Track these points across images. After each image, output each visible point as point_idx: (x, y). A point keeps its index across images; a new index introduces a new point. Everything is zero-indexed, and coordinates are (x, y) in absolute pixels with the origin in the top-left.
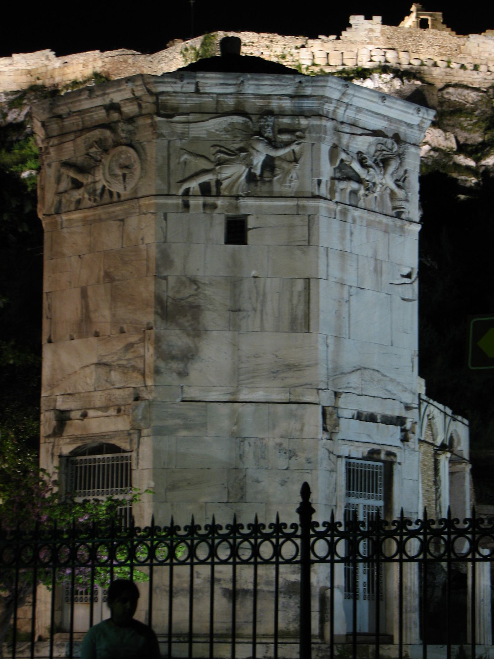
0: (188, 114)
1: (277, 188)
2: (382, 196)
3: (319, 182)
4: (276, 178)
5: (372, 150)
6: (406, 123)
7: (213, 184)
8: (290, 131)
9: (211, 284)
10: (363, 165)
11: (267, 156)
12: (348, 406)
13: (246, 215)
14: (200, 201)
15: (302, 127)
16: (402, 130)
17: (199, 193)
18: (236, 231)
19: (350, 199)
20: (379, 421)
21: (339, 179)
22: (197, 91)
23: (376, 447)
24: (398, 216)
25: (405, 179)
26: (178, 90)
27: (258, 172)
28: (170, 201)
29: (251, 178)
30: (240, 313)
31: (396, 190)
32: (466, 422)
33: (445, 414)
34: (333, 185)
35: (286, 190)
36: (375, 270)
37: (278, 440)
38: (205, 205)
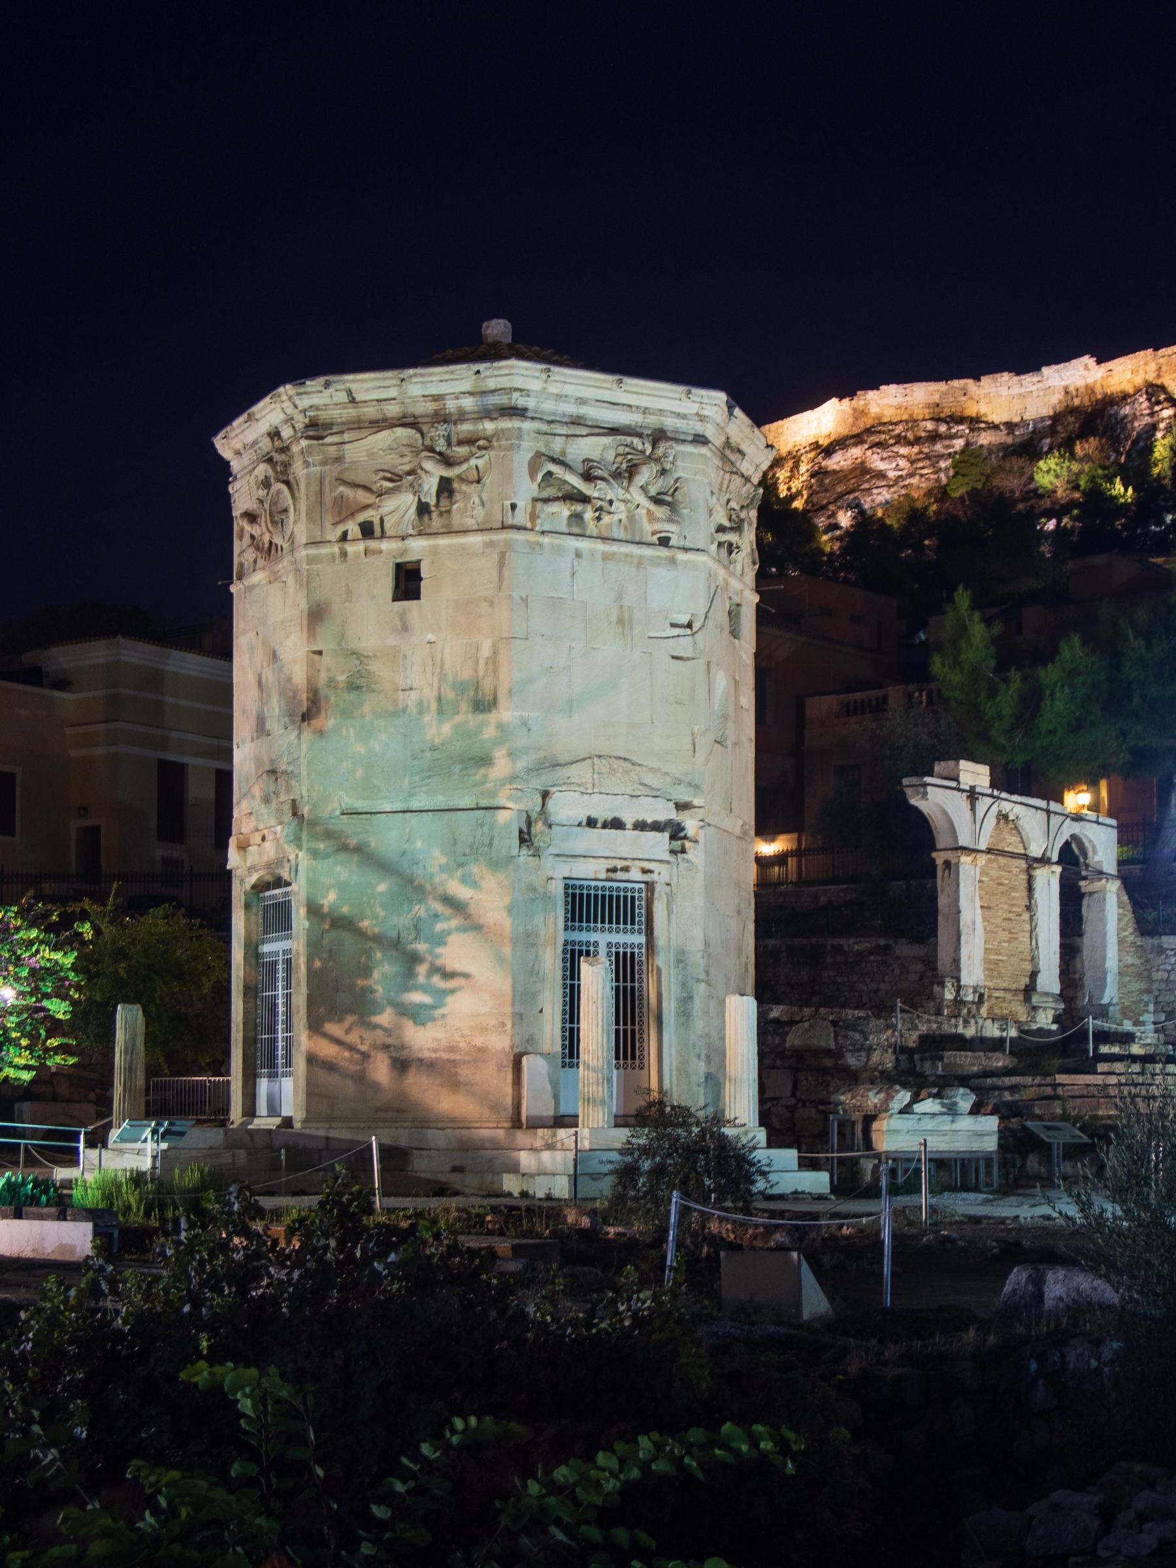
0: (342, 432)
1: (457, 520)
2: (631, 518)
3: (513, 507)
4: (455, 507)
5: (610, 456)
6: (672, 412)
7: (376, 521)
8: (470, 442)
9: (375, 656)
10: (588, 477)
11: (442, 478)
12: (567, 807)
13: (419, 562)
14: (361, 546)
15: (489, 433)
16: (670, 423)
17: (360, 536)
18: (408, 582)
19: (569, 525)
20: (629, 826)
21: (546, 501)
22: (353, 401)
23: (620, 864)
24: (664, 542)
25: (676, 490)
26: (327, 401)
27: (432, 501)
28: (324, 551)
29: (423, 509)
30: (412, 692)
31: (652, 507)
32: (1114, 822)
33: (1048, 812)
34: (534, 508)
35: (470, 523)
36: (620, 621)
37: (461, 859)
38: (366, 552)
